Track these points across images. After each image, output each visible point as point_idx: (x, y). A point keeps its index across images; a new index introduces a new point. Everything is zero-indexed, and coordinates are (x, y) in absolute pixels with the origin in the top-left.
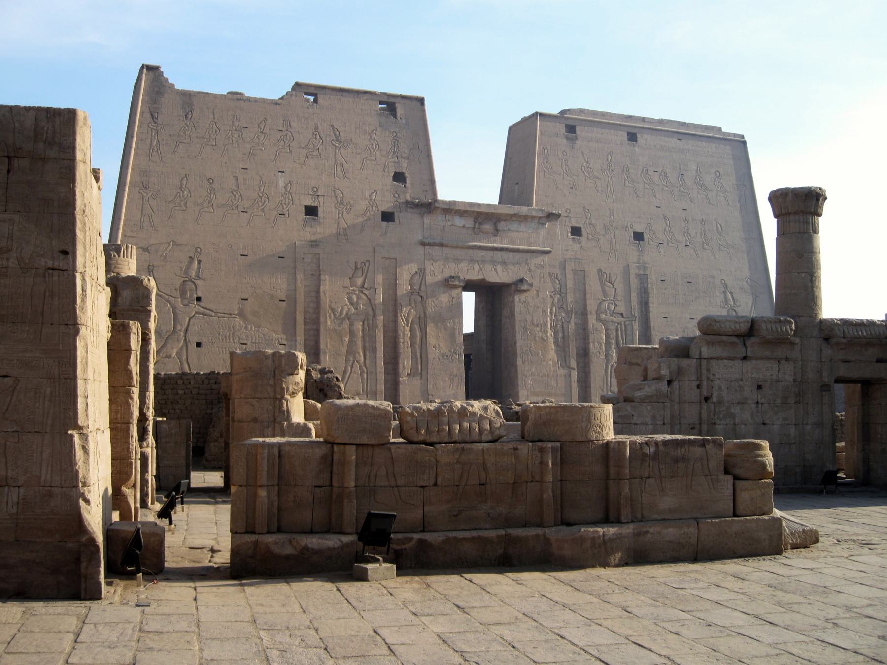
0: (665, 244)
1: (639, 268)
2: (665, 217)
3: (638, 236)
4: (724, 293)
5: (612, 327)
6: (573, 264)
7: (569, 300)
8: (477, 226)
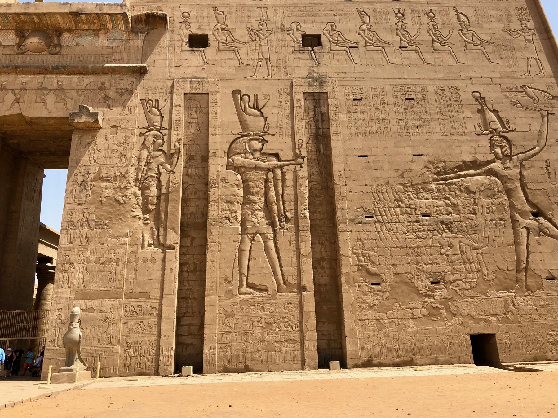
0: (361, 49)
1: (310, 85)
2: (360, 12)
3: (312, 41)
4: (481, 111)
5: (257, 178)
6: (187, 85)
7: (174, 138)
8: (18, 39)
